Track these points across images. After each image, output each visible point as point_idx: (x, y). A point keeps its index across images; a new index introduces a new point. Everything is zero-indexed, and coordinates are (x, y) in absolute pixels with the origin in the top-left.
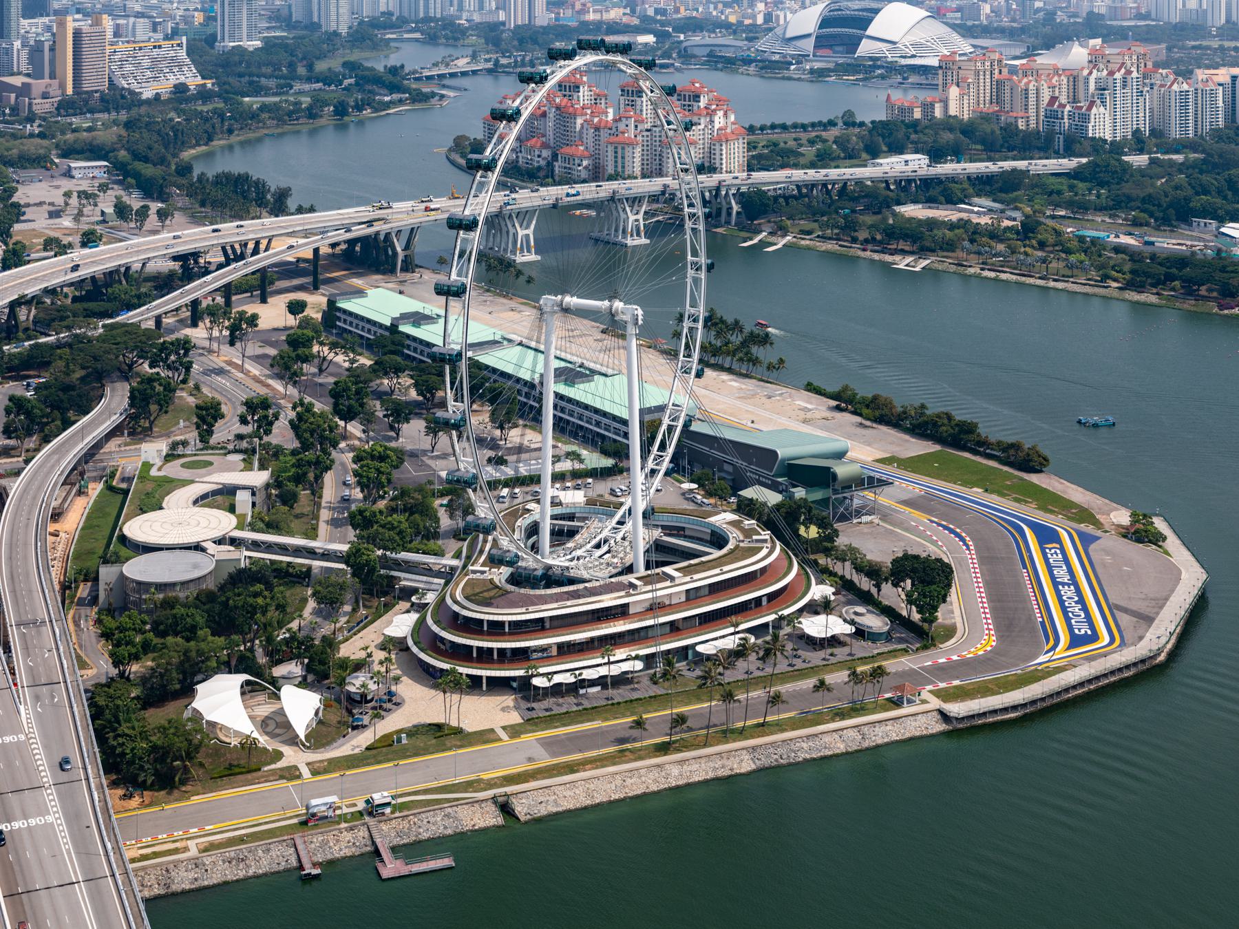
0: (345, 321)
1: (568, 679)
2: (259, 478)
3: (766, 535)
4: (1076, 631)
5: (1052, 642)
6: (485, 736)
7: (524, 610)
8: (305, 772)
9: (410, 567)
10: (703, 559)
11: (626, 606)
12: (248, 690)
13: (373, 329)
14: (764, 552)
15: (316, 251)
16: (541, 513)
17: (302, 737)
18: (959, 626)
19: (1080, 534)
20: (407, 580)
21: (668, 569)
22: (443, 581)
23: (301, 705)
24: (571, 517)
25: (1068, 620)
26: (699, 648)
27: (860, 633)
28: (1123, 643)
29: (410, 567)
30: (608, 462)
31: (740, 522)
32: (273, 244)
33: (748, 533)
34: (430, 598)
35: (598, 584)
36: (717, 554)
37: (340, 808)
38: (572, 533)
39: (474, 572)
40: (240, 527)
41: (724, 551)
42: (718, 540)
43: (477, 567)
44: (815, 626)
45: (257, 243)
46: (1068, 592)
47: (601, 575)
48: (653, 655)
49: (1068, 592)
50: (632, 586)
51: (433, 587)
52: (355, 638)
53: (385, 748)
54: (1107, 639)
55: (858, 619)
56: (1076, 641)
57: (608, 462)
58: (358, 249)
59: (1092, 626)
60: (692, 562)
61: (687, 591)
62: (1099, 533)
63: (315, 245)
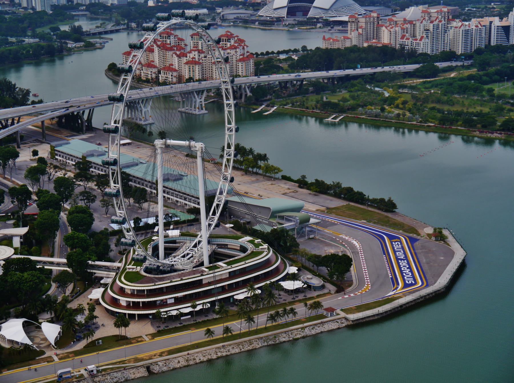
0: (60, 156)
1: (174, 313)
2: (23, 230)
3: (266, 246)
4: (407, 282)
5: (396, 286)
6: (138, 339)
7: (153, 284)
8: (56, 358)
9: (99, 268)
10: (236, 258)
11: (202, 280)
12: (25, 325)
13: (74, 159)
14: (265, 253)
15: (43, 122)
16: (160, 241)
17: (53, 343)
18: (354, 281)
19: (410, 238)
20: (99, 273)
21: (220, 263)
22: (115, 274)
23: (51, 331)
24: (174, 242)
25: (403, 277)
26: (235, 297)
27: (309, 287)
28: (427, 286)
29: (99, 268)
30: (192, 217)
31: (254, 241)
32: (21, 120)
34: (109, 281)
35: (188, 271)
36: (243, 255)
37: (73, 373)
38: (175, 249)
39: (129, 269)
40: (15, 253)
41: (246, 254)
42: (243, 249)
43: (130, 267)
44: (289, 285)
45: (13, 120)
46: (403, 263)
47: (189, 267)
48: (214, 301)
49: (403, 263)
50: (203, 271)
51: (110, 276)
52: (75, 300)
53: (92, 347)
54: (420, 284)
55: (308, 281)
56: (406, 285)
57: (192, 217)
58: (63, 120)
59: (415, 280)
60: (231, 259)
61: (230, 272)
62: (419, 237)
63: (42, 120)
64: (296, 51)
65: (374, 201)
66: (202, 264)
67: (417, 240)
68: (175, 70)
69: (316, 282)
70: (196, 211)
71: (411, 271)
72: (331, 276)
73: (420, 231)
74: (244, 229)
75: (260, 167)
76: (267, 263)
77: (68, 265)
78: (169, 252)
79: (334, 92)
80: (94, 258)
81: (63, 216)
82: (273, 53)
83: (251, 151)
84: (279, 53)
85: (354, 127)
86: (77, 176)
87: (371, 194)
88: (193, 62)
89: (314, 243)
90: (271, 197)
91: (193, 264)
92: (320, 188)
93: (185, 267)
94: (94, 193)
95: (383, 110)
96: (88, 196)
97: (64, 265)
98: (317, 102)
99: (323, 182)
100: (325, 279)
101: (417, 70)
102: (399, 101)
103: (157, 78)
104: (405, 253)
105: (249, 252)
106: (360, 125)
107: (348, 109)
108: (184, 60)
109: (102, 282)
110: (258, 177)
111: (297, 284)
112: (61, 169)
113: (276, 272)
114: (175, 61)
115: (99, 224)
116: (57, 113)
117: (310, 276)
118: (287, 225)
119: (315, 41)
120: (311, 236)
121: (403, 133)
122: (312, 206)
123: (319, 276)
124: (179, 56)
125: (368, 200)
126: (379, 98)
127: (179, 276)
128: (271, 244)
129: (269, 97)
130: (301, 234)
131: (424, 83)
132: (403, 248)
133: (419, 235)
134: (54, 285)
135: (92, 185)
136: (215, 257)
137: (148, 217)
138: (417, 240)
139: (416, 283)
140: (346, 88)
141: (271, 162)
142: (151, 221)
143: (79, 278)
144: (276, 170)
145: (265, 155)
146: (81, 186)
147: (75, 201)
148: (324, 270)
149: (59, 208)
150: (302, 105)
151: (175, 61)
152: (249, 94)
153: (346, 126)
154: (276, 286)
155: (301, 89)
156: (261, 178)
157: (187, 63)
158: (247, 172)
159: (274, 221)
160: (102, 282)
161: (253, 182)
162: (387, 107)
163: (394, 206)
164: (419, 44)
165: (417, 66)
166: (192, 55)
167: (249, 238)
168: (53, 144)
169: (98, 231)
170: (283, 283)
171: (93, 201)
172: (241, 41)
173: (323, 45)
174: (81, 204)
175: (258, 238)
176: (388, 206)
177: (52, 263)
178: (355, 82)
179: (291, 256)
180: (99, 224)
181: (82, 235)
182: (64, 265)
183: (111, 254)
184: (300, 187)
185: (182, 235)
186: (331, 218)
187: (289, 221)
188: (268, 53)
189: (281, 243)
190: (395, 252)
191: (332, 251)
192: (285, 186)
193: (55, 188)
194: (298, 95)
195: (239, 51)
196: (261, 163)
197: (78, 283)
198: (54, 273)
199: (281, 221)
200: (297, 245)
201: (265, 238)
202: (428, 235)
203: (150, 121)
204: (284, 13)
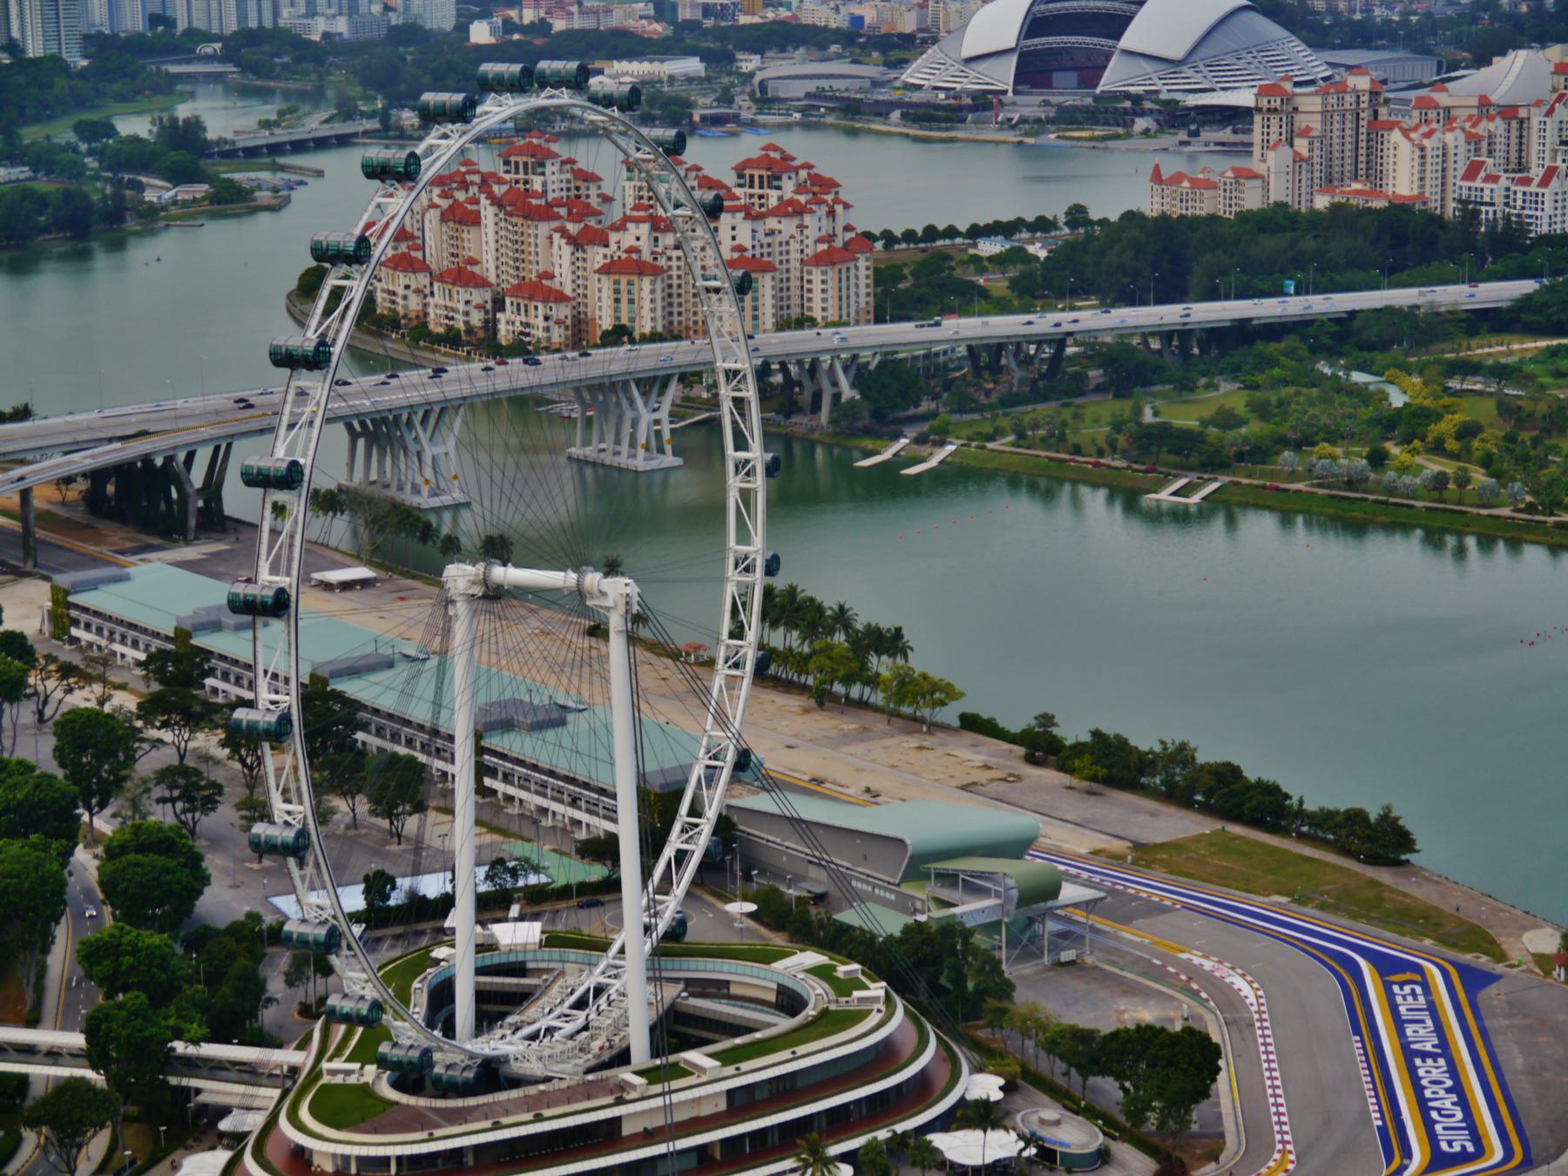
0: (88, 627)
3: (877, 989)
4: (1444, 1146)
5: (1397, 1161)
7: (424, 1135)
9: (216, 1068)
10: (758, 1035)
11: (617, 1121)
13: (143, 638)
15: (25, 494)
18: (1230, 1138)
19: (1463, 969)
20: (213, 1091)
21: (695, 1056)
22: (276, 1093)
24: (519, 969)
25: (1429, 1124)
29: (216, 1068)
30: (595, 872)
31: (834, 968)
33: (844, 987)
34: (253, 1122)
35: (564, 1085)
36: (784, 1023)
38: (519, 998)
39: (333, 1072)
41: (799, 1019)
42: (789, 1002)
47: (570, 1071)
50: (623, 1087)
51: (256, 1103)
54: (1498, 1154)
55: (1043, 1132)
57: (595, 872)
58: (110, 489)
59: (1476, 1138)
60: (738, 1041)
61: (730, 1093)
62: (1500, 968)
64: (1043, 225)
65: (1324, 819)
66: (623, 1058)
67: (1492, 978)
68: (561, 298)
69: (1075, 1136)
70: (604, 850)
71: (1464, 1103)
72: (1136, 1111)
73: (1506, 943)
74: (797, 921)
75: (873, 681)
76: (883, 1057)
77: (94, 1056)
78: (495, 1007)
79: (1185, 386)
80: (195, 1029)
81: (85, 860)
82: (951, 232)
83: (842, 617)
84: (976, 232)
85: (1260, 527)
86: (151, 708)
87: (1314, 789)
88: (629, 267)
89: (1072, 983)
90: (913, 797)
91: (589, 1059)
92: (1111, 765)
93: (555, 1069)
94: (217, 775)
95: (1378, 459)
96: (189, 784)
97: (75, 1056)
98: (1118, 426)
99: (1122, 743)
100: (1110, 1126)
101: (1526, 302)
102: (1445, 427)
103: (491, 326)
104: (1440, 1030)
105: (810, 1012)
106: (1286, 521)
107: (1240, 457)
108: (597, 256)
109: (225, 1125)
110: (868, 718)
111: (1000, 1145)
112: (89, 679)
113: (920, 1091)
114: (561, 260)
115: (223, 900)
116: (84, 461)
117: (1051, 1112)
118: (970, 909)
119: (1123, 185)
120: (1067, 955)
121: (1460, 552)
122: (1074, 833)
123: (1090, 1113)
124: (577, 243)
125: (1301, 814)
126: (1366, 412)
127: (529, 1104)
128: (899, 984)
129: (926, 406)
130: (1025, 943)
131: (1554, 353)
132: (1432, 1008)
133: (1501, 957)
134: (30, 1139)
135: (207, 741)
136: (676, 1030)
137: (416, 872)
138: (1492, 978)
139: (1480, 1152)
140: (1234, 372)
141: (921, 661)
142: (431, 886)
143: (133, 1110)
144: (936, 691)
145: (898, 633)
146: (163, 745)
147: (135, 804)
148: (1109, 1090)
149: (68, 832)
150: (1057, 439)
151: (561, 260)
152: (848, 392)
153: (1231, 522)
154: (913, 1148)
155: (1057, 373)
156: (878, 723)
157: (605, 270)
158: (823, 699)
159: (919, 892)
160: (225, 1125)
161: (846, 738)
162: (1393, 449)
163: (1404, 840)
164: (1536, 200)
165: (1528, 286)
166: (628, 240)
167: (812, 958)
168: (63, 580)
169: (222, 923)
170: (938, 1140)
171: (209, 804)
172: (821, 185)
173: (1150, 203)
174: (162, 816)
175: (852, 958)
176: (1384, 841)
177: (27, 1052)
178: (1273, 348)
179: (981, 1034)
180: (223, 900)
181: (153, 939)
182: (75, 1056)
183: (268, 1015)
184: (1031, 760)
185: (552, 940)
186: (1147, 887)
187: (982, 892)
188: (931, 233)
189: (943, 981)
190: (1399, 1024)
191: (1147, 1014)
192: (973, 754)
193: (60, 754)
194: (1044, 398)
195: (815, 224)
196: (881, 665)
197: (129, 1132)
198: (37, 1090)
199: (945, 894)
200: (1006, 989)
201: (879, 957)
202: (1541, 960)
203: (458, 496)
204: (1003, 75)
